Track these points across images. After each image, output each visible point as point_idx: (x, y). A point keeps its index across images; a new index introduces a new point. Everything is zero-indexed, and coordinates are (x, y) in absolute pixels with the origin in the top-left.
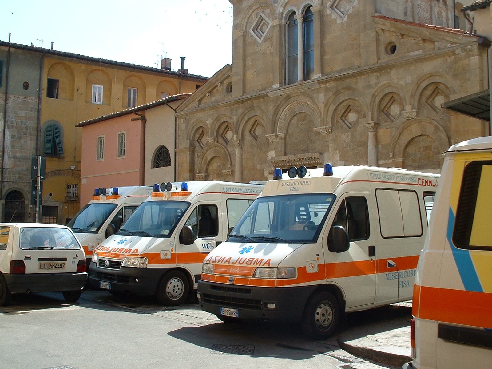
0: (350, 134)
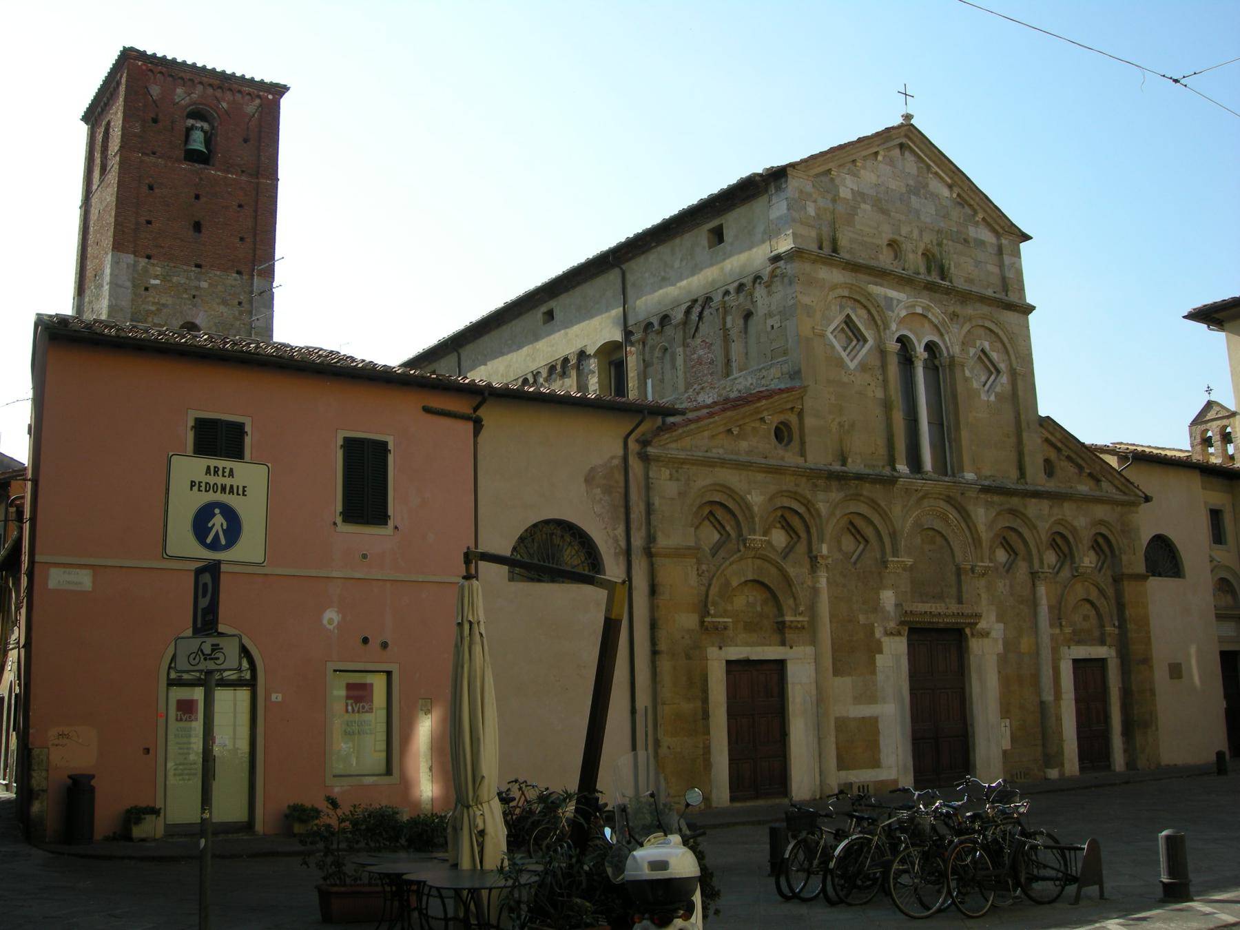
0: (1007, 582)
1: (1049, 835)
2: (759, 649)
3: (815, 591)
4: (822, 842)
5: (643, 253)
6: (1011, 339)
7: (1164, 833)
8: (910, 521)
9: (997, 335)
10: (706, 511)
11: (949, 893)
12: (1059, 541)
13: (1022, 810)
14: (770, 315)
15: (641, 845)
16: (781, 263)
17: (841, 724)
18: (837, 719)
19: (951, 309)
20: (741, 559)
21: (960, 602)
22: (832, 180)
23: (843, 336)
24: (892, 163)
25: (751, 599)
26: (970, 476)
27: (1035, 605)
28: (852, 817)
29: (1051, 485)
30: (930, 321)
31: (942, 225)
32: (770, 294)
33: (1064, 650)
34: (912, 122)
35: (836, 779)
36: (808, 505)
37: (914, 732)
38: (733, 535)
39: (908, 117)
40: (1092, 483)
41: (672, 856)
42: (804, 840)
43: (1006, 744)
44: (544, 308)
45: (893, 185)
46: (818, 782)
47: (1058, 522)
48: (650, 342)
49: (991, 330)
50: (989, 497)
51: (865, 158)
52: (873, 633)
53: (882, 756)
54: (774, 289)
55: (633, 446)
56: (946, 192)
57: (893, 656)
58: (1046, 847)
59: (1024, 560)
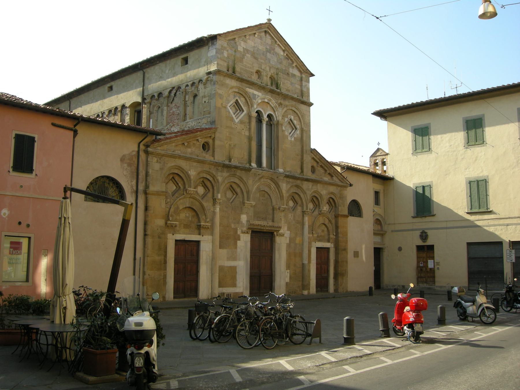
1: (301, 317)
2: (189, 236)
3: (214, 213)
4: (210, 317)
5: (153, 65)
6: (302, 116)
7: (346, 318)
8: (256, 187)
9: (297, 114)
10: (171, 177)
11: (260, 339)
12: (315, 199)
13: (291, 307)
14: (204, 97)
15: (132, 315)
16: (211, 75)
17: (221, 268)
18: (220, 266)
19: (279, 101)
20: (184, 198)
21: (273, 221)
22: (236, 43)
23: (234, 109)
24: (261, 38)
25: (187, 215)
26: (281, 170)
27: (303, 224)
28: (222, 307)
29: (313, 177)
30: (270, 105)
31: (279, 66)
32: (205, 88)
33: (313, 243)
34: (271, 22)
35: (218, 291)
36: (214, 177)
37: (251, 273)
38: (182, 187)
39: (269, 20)
40: (329, 177)
41: (145, 321)
42: (202, 316)
43: (288, 280)
44: (109, 85)
45: (260, 47)
46: (210, 292)
47: (315, 192)
48: (153, 104)
49: (295, 112)
50: (288, 180)
51: (250, 35)
52: (237, 232)
53: (237, 282)
54: (207, 86)
55: (142, 147)
56: (282, 53)
57: (245, 241)
58: (299, 322)
59: (300, 206)
